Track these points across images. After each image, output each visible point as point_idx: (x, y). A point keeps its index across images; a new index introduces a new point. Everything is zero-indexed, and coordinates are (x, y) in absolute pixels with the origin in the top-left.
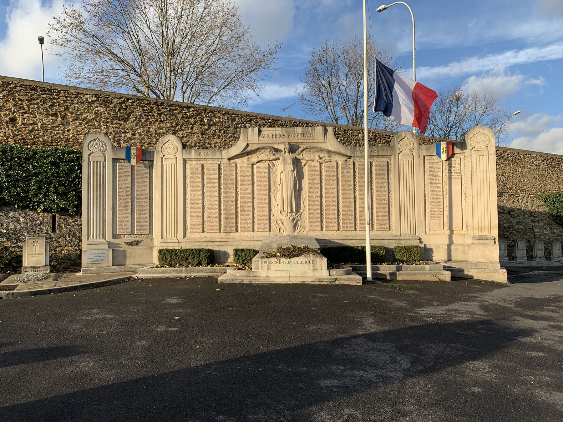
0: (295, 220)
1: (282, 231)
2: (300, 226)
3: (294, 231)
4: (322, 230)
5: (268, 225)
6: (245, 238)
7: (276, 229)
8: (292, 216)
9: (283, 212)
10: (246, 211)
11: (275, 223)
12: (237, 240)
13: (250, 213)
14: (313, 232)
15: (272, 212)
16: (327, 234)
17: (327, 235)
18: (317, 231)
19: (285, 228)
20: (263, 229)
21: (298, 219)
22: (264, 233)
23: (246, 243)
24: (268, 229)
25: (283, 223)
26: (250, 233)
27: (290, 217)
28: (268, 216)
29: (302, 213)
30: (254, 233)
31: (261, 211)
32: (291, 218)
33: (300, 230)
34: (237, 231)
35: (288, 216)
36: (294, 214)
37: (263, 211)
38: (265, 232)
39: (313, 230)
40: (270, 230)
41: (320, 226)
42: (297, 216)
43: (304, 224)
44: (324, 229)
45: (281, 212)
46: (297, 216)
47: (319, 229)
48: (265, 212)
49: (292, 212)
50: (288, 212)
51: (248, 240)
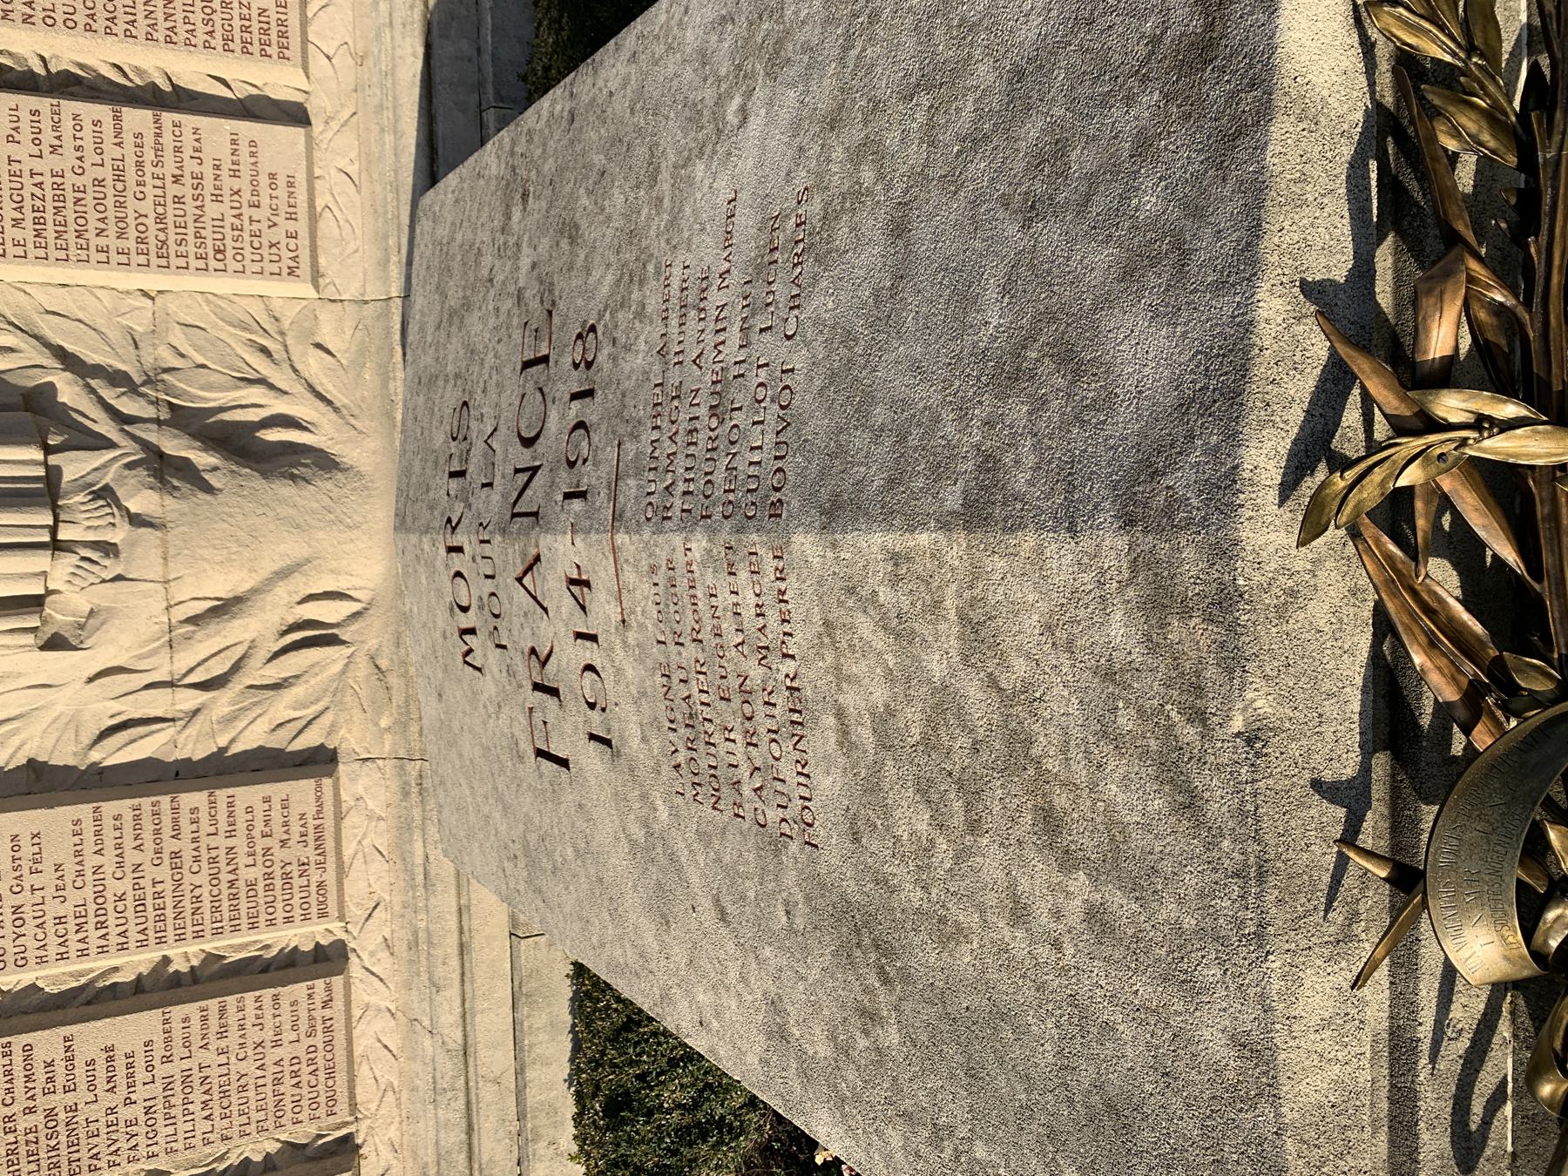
0: (174, 445)
1: (328, 612)
2: (255, 394)
3: (325, 462)
4: (295, 115)
5: (248, 795)
6: (427, 1042)
7: (298, 691)
8: (105, 494)
9: (59, 616)
10: (59, 1100)
11: (222, 702)
12: (455, 1137)
13: (84, 1051)
14: (326, 226)
15: (65, 755)
16: (343, 61)
17: (361, 60)
18: (311, 178)
19: (283, 574)
20: (310, 853)
21: (149, 412)
22: (353, 822)
23: (493, 1022)
24: (307, 785)
25: (224, 608)
26: (360, 994)
27: (136, 520)
28: (123, 806)
29: (68, 361)
30: (367, 946)
31: (53, 909)
32: (142, 501)
33: (298, 388)
34: (348, 1138)
35: (109, 549)
36: (75, 466)
37: (47, 879)
38: (339, 817)
39: (302, 227)
40: (320, 761)
41: (248, 129)
42: (106, 427)
43: (227, 333)
44: (280, 82)
45: (56, 643)
46: (106, 427)
47: (279, 140)
48: (59, 850)
49: (48, 491)
50: (57, 546)
51: (449, 1019)
